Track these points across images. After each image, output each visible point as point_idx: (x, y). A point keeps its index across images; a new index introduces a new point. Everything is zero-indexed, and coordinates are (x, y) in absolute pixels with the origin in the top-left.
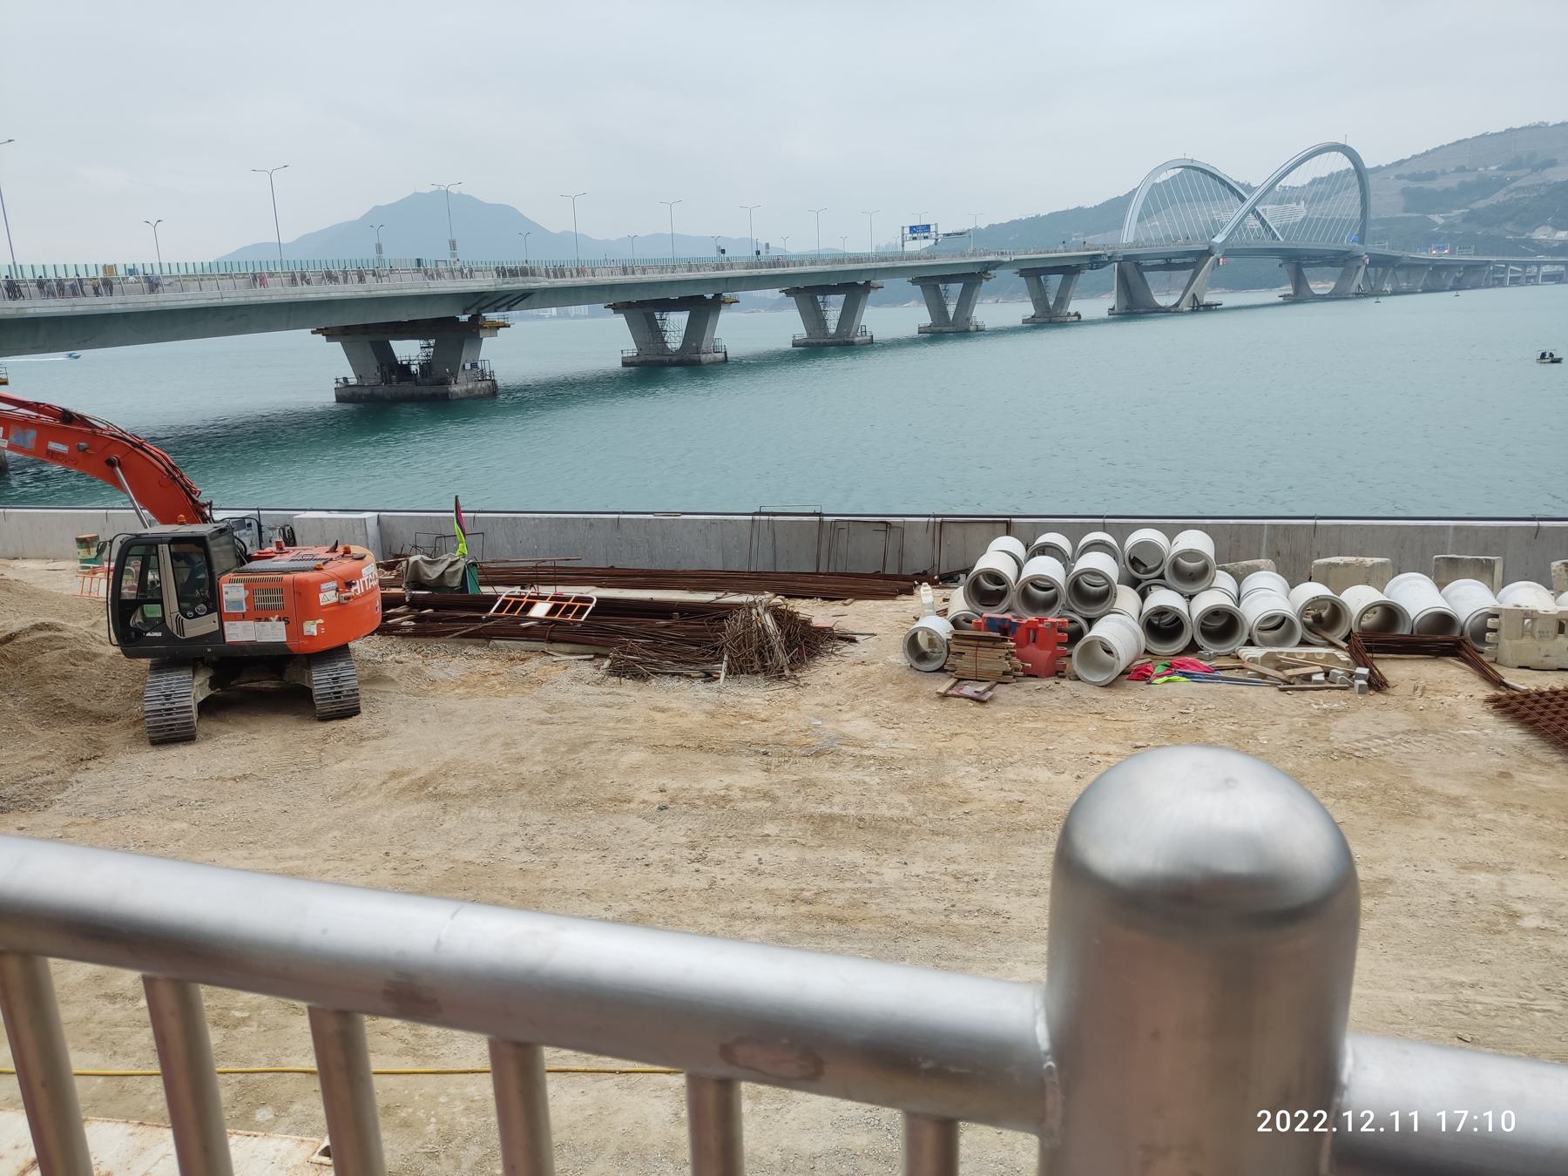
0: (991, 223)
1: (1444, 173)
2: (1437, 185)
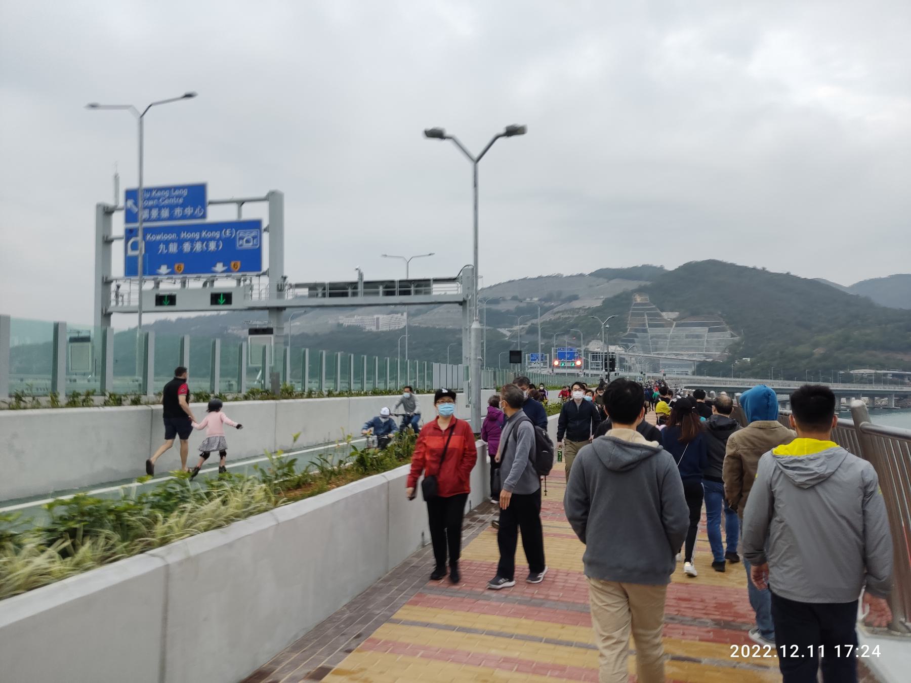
1: (504, 300)
2: (502, 307)
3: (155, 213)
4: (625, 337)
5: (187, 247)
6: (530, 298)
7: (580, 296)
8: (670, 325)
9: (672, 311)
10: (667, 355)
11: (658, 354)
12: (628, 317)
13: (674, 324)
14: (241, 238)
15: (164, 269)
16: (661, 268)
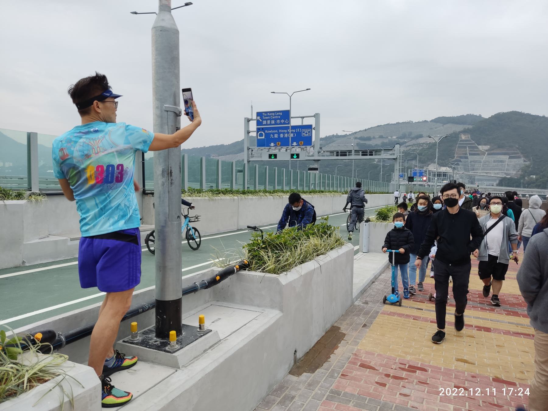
0: (184, 148)
1: (374, 138)
2: (373, 143)
3: (269, 122)
4: (453, 161)
5: (282, 135)
6: (391, 137)
7: (423, 135)
8: (483, 154)
9: (485, 145)
10: (480, 173)
11: (474, 172)
12: (455, 149)
13: (486, 154)
14: (304, 132)
15: (272, 144)
16: (480, 116)
